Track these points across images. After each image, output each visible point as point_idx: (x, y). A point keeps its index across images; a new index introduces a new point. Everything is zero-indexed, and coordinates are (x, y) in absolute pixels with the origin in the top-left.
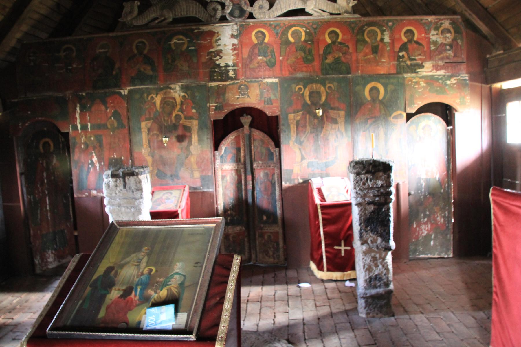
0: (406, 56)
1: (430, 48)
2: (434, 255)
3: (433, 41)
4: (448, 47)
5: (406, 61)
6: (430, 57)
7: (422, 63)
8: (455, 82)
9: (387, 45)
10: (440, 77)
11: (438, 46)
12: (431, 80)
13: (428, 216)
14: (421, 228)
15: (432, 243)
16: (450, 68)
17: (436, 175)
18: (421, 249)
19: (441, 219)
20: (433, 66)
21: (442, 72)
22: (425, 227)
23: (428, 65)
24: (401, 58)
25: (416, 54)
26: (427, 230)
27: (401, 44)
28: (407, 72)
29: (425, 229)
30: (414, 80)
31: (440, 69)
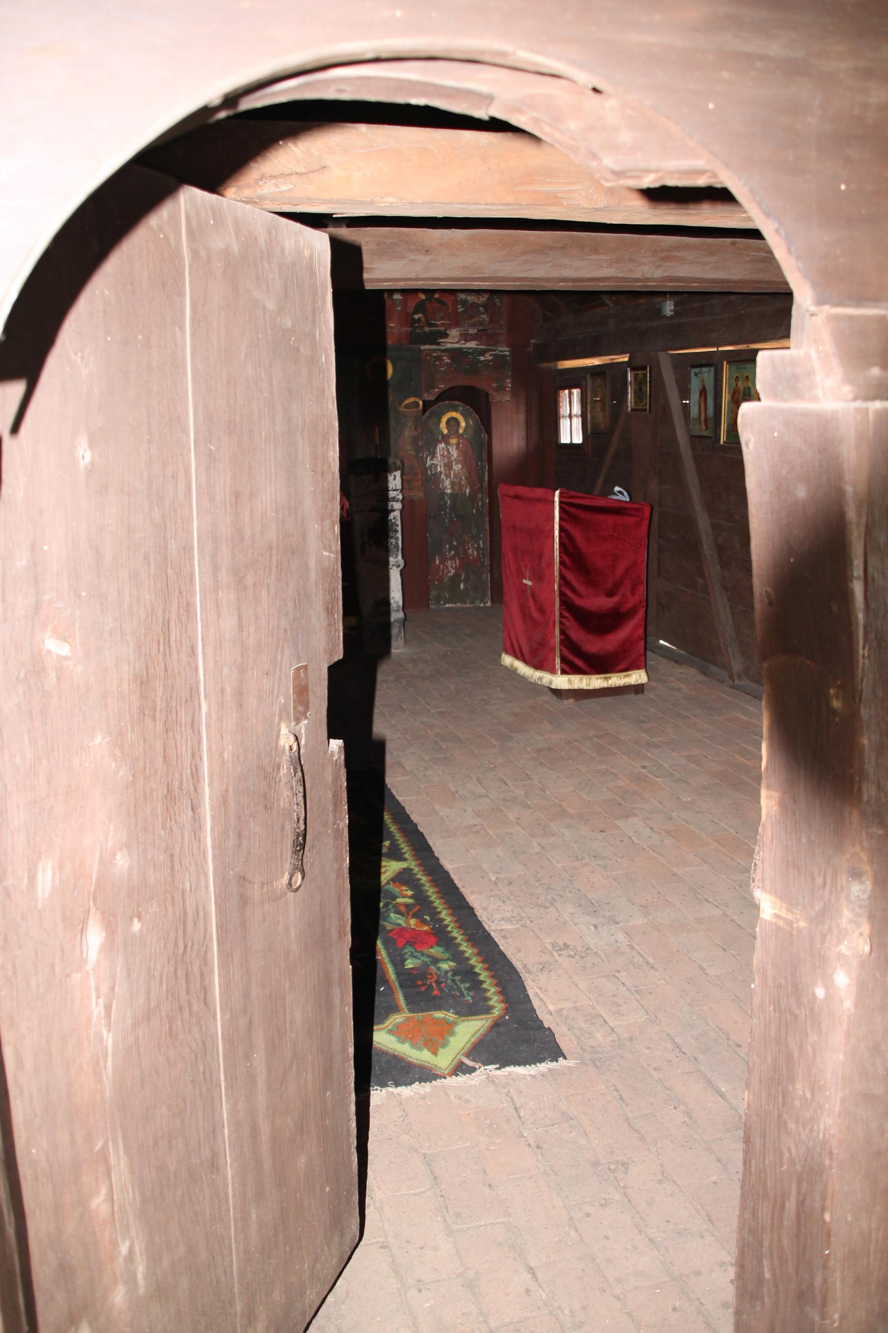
0: (423, 320)
1: (457, 309)
2: (465, 603)
3: (462, 299)
4: (481, 309)
5: (423, 327)
6: (456, 323)
7: (446, 330)
8: (490, 358)
9: (397, 303)
10: (470, 351)
11: (468, 306)
12: (456, 354)
13: (456, 548)
14: (446, 566)
15: (462, 586)
16: (484, 338)
17: (466, 488)
18: (447, 595)
19: (473, 552)
20: (461, 335)
21: (472, 345)
22: (452, 564)
23: (454, 333)
24: (416, 323)
25: (438, 317)
26: (455, 568)
27: (417, 302)
28: (425, 343)
29: (452, 567)
30: (434, 354)
31: (470, 340)
